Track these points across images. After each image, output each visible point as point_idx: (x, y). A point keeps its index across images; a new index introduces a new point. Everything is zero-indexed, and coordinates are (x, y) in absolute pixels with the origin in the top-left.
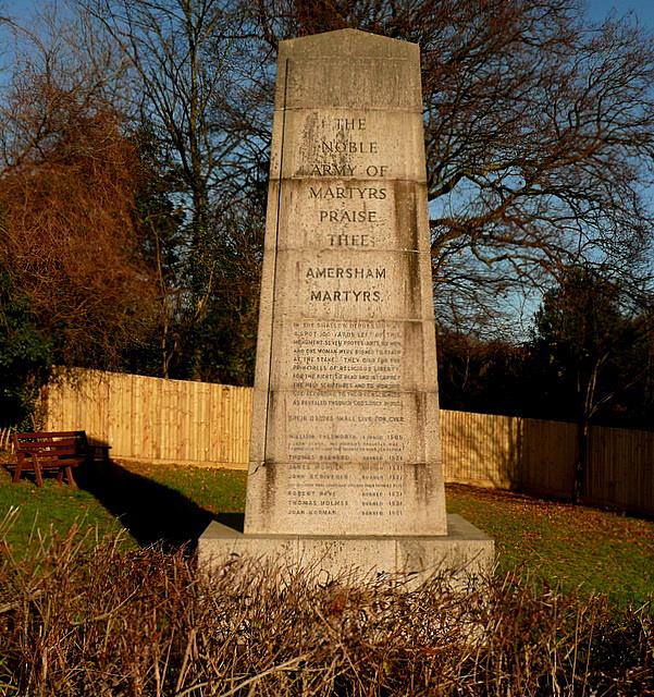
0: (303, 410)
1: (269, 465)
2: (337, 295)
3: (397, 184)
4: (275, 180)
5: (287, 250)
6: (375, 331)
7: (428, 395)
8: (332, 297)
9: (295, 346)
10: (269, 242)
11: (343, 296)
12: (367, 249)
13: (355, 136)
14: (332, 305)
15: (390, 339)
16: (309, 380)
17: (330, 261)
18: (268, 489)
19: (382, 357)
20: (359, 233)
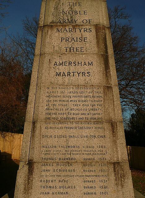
0: (50, 132)
1: (30, 164)
2: (69, 74)
3: (97, 27)
4: (41, 27)
5: (45, 54)
6: (89, 91)
7: (118, 123)
8: (66, 74)
9: (47, 99)
10: (37, 52)
11: (72, 74)
12: (83, 53)
13: (77, 8)
14: (66, 79)
15: (97, 95)
16: (54, 116)
17: (65, 59)
18: (29, 179)
19: (93, 103)
20: (79, 46)
